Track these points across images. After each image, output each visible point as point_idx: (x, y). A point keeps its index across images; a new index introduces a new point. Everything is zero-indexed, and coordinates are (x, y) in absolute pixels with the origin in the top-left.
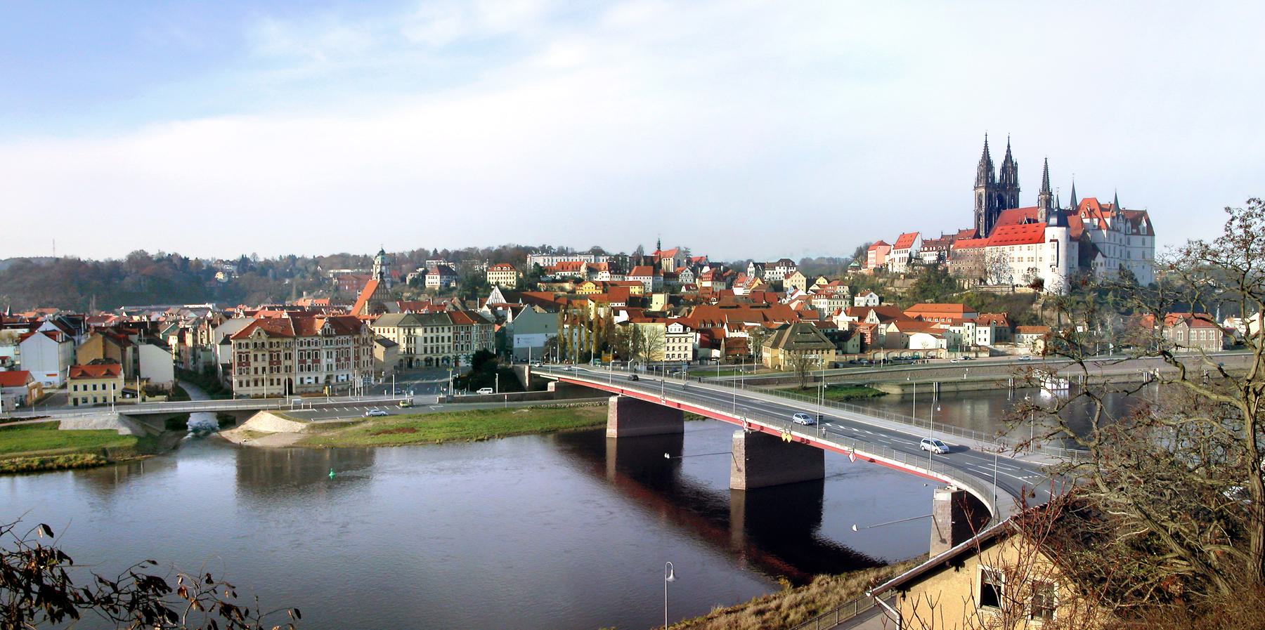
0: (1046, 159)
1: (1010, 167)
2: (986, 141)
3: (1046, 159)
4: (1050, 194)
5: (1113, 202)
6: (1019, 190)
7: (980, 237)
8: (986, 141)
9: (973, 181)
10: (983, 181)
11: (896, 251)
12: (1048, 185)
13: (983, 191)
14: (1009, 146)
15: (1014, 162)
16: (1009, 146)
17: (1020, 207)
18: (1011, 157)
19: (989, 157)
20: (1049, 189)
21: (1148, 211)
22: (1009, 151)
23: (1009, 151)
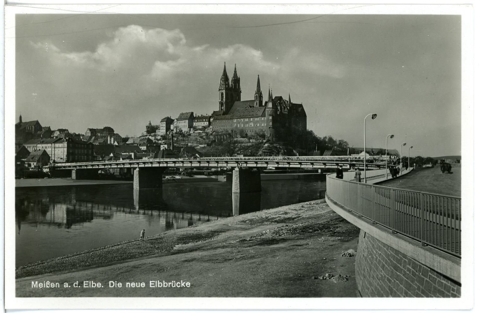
0: (258, 75)
1: (237, 80)
2: (225, 66)
3: (258, 75)
4: (261, 94)
5: (288, 100)
6: (241, 92)
8: (225, 66)
9: (218, 87)
10: (223, 87)
12: (260, 89)
13: (224, 91)
14: (235, 69)
15: (238, 77)
16: (235, 69)
17: (242, 100)
18: (237, 74)
19: (227, 74)
20: (260, 91)
21: (302, 104)
22: (235, 72)
23: (235, 72)
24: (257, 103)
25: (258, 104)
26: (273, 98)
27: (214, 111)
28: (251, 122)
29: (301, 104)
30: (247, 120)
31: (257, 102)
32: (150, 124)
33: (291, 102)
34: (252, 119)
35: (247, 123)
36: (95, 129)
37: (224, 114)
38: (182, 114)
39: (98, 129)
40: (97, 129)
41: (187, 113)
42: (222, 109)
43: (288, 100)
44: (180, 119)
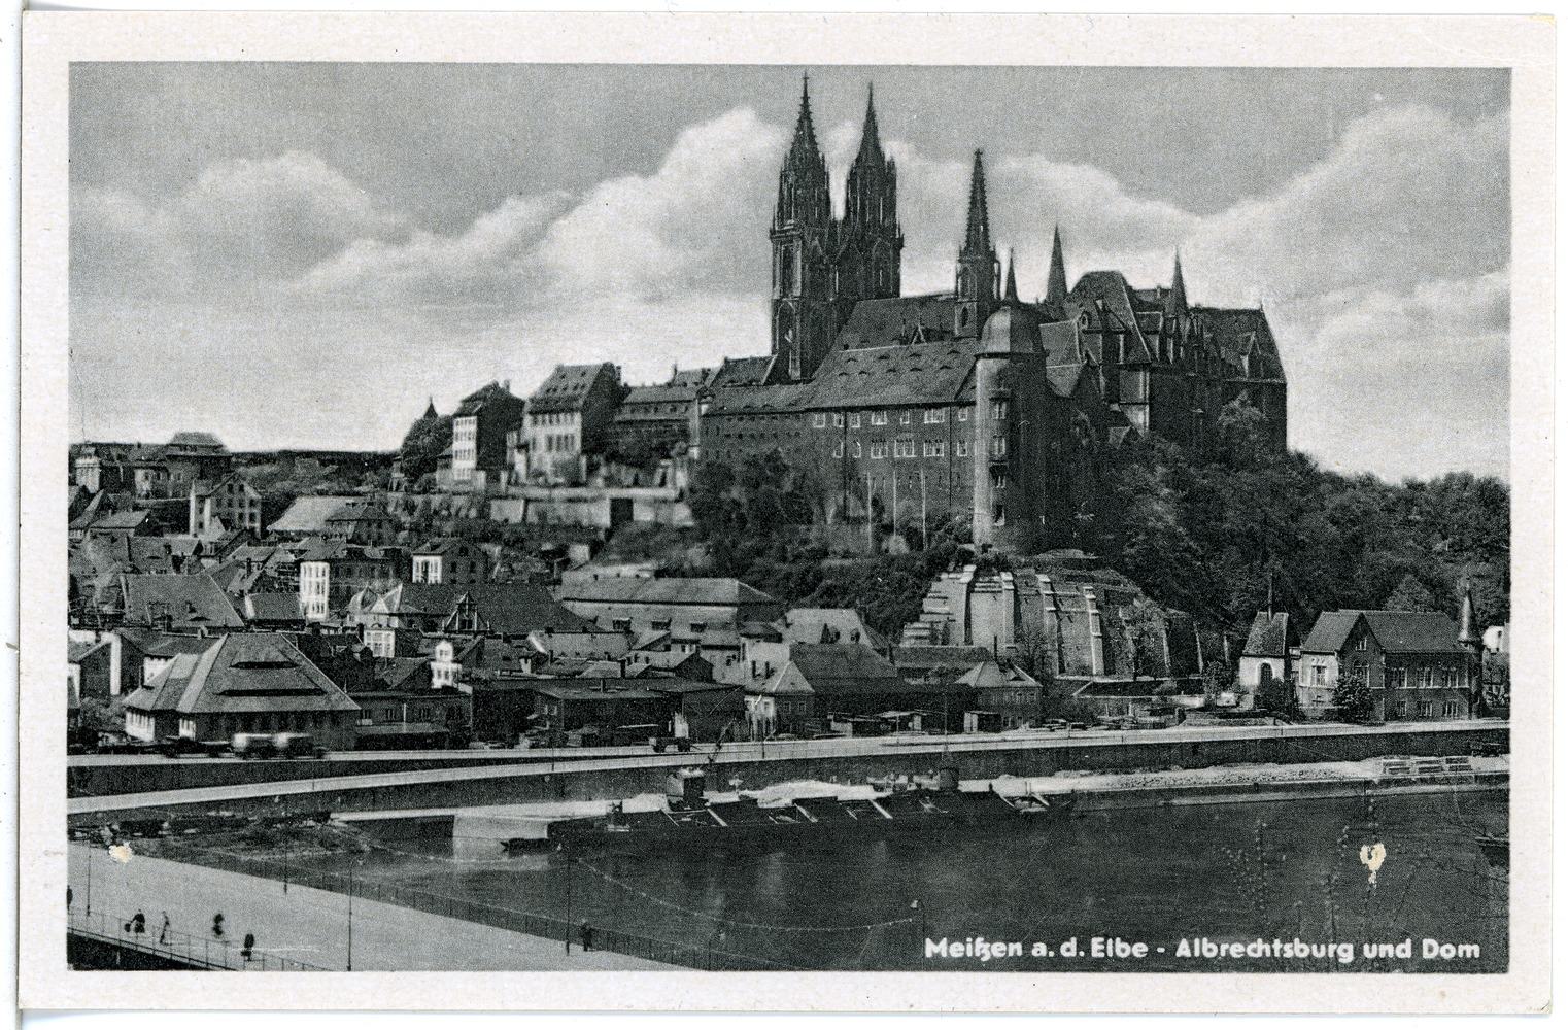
2: (805, 98)
4: (992, 257)
7: (790, 382)
11: (540, 417)
24: (965, 310)
25: (972, 316)
26: (1072, 279)
27: (727, 361)
28: (901, 430)
29: (1255, 307)
30: (879, 421)
31: (968, 305)
32: (431, 412)
33: (1191, 302)
34: (905, 420)
35: (879, 438)
36: (131, 446)
37: (779, 376)
38: (561, 373)
39: (149, 446)
40: (139, 446)
41: (583, 371)
42: (781, 347)
43: (1168, 284)
44: (548, 405)
